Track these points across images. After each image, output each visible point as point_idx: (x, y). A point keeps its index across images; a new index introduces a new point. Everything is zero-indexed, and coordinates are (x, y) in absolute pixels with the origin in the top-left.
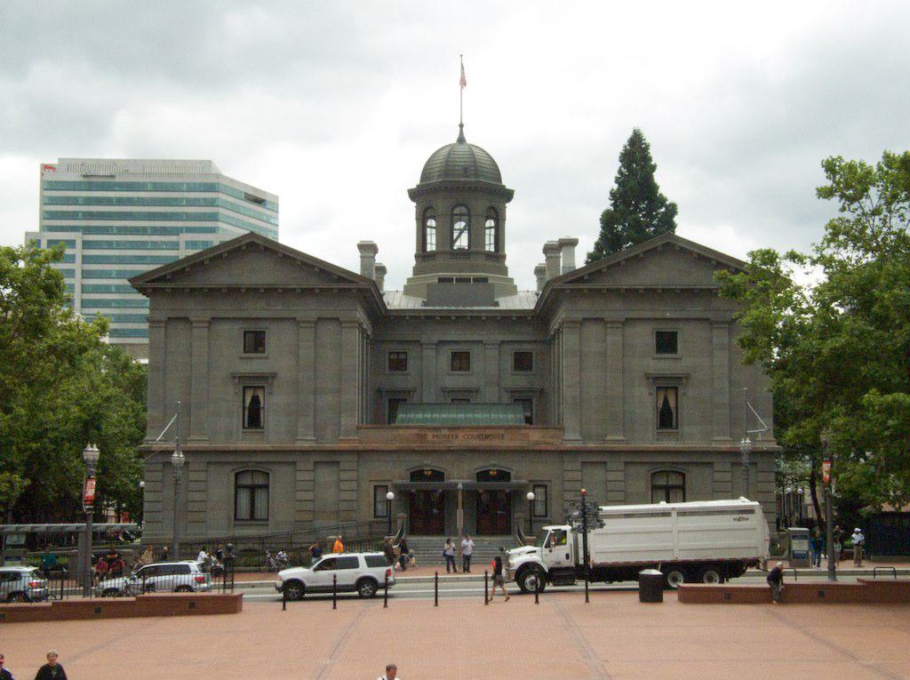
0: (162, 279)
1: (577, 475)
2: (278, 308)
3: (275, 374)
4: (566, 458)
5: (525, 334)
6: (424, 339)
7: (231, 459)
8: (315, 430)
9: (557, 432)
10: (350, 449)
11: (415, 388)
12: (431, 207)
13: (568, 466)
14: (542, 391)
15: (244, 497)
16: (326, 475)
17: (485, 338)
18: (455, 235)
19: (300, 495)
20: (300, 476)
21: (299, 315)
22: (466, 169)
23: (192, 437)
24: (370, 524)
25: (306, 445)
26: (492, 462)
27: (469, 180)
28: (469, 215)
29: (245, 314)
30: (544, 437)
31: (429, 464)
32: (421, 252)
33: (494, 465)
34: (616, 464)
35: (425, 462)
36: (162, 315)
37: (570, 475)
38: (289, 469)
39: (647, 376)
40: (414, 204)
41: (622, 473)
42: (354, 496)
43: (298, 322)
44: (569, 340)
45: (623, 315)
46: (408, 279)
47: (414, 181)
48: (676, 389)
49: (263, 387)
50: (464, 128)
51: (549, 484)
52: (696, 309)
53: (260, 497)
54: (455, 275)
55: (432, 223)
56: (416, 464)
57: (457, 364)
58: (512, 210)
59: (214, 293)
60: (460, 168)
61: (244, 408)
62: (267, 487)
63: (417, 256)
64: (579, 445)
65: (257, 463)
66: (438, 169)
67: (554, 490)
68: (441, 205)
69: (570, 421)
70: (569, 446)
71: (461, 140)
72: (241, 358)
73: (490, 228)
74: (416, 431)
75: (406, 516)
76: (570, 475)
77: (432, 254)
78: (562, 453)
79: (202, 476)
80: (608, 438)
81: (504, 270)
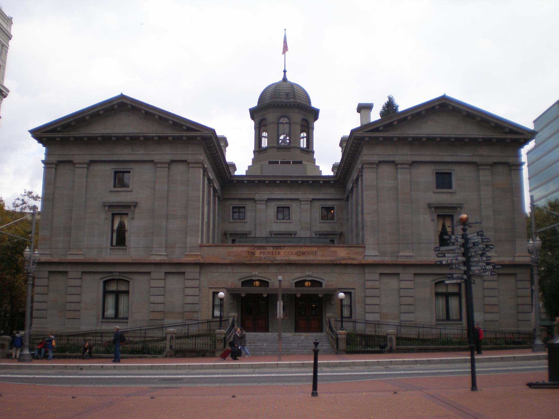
0: (54, 130)
1: (377, 284)
2: (140, 153)
3: (137, 203)
4: (367, 270)
5: (329, 193)
6: (257, 197)
7: (101, 269)
8: (166, 247)
9: (360, 250)
10: (193, 262)
11: (251, 232)
12: (265, 119)
13: (368, 276)
14: (341, 234)
15: (111, 300)
16: (174, 283)
17: (300, 196)
19: (153, 299)
20: (154, 283)
21: (156, 158)
22: (287, 95)
23: (71, 252)
24: (208, 322)
25: (158, 259)
26: (307, 273)
27: (289, 100)
28: (289, 123)
29: (115, 158)
30: (348, 254)
31: (257, 274)
32: (257, 149)
33: (309, 276)
34: (407, 274)
35: (253, 273)
36: (54, 159)
37: (369, 284)
38: (145, 278)
39: (430, 206)
41: (412, 282)
42: (196, 299)
43: (156, 163)
44: (368, 177)
45: (410, 159)
46: (249, 167)
47: (254, 104)
48: (451, 217)
49: (127, 214)
50: (287, 73)
51: (352, 291)
52: (465, 155)
53: (123, 300)
55: (265, 134)
56: (246, 275)
57: (281, 216)
58: (317, 125)
59: (92, 141)
60: (284, 94)
61: (112, 231)
62: (127, 292)
63: (254, 152)
64: (378, 259)
65: (120, 273)
66: (269, 95)
67: (358, 295)
68: (271, 117)
69: (369, 240)
70: (369, 260)
71: (285, 79)
72: (111, 191)
73: (303, 138)
74: (246, 249)
75: (236, 315)
76: (369, 284)
77: (266, 149)
78: (363, 266)
79: (78, 282)
80: (401, 254)
81: (314, 161)
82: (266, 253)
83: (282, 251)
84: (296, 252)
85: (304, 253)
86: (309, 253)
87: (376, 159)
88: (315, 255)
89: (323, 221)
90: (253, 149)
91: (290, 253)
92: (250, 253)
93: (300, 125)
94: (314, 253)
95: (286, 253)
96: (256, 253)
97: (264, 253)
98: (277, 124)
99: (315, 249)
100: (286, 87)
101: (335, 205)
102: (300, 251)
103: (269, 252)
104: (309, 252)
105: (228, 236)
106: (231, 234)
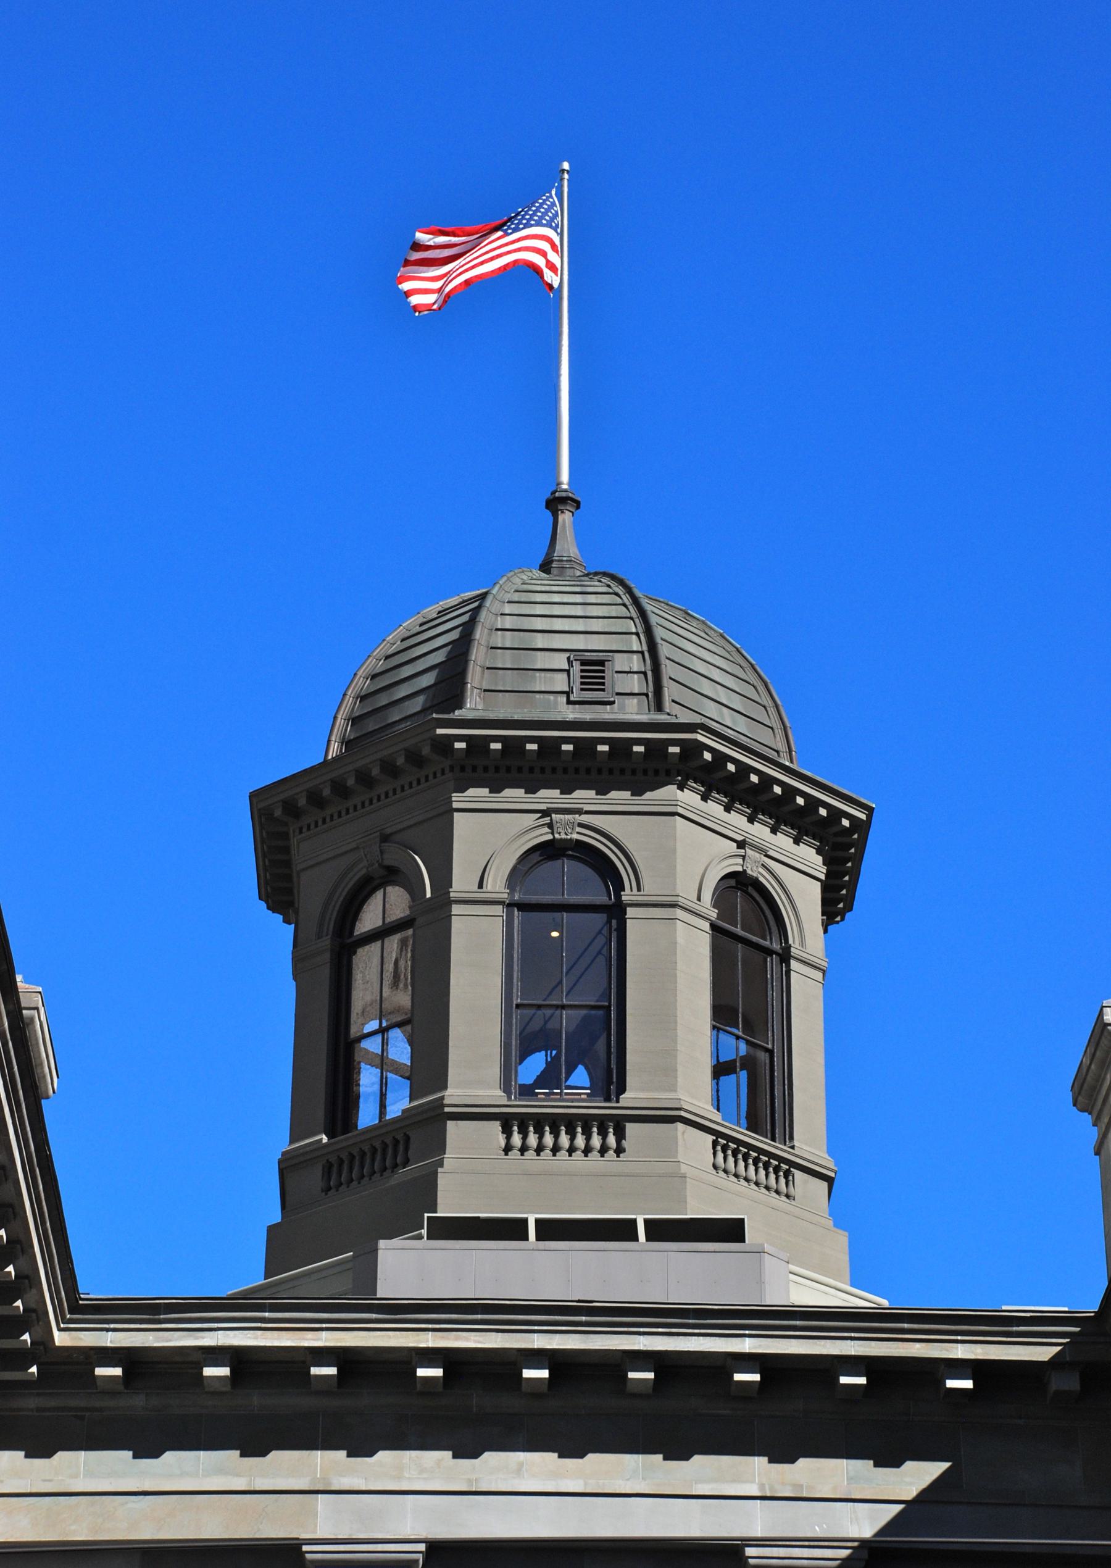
60: (560, 660)
93: (706, 926)
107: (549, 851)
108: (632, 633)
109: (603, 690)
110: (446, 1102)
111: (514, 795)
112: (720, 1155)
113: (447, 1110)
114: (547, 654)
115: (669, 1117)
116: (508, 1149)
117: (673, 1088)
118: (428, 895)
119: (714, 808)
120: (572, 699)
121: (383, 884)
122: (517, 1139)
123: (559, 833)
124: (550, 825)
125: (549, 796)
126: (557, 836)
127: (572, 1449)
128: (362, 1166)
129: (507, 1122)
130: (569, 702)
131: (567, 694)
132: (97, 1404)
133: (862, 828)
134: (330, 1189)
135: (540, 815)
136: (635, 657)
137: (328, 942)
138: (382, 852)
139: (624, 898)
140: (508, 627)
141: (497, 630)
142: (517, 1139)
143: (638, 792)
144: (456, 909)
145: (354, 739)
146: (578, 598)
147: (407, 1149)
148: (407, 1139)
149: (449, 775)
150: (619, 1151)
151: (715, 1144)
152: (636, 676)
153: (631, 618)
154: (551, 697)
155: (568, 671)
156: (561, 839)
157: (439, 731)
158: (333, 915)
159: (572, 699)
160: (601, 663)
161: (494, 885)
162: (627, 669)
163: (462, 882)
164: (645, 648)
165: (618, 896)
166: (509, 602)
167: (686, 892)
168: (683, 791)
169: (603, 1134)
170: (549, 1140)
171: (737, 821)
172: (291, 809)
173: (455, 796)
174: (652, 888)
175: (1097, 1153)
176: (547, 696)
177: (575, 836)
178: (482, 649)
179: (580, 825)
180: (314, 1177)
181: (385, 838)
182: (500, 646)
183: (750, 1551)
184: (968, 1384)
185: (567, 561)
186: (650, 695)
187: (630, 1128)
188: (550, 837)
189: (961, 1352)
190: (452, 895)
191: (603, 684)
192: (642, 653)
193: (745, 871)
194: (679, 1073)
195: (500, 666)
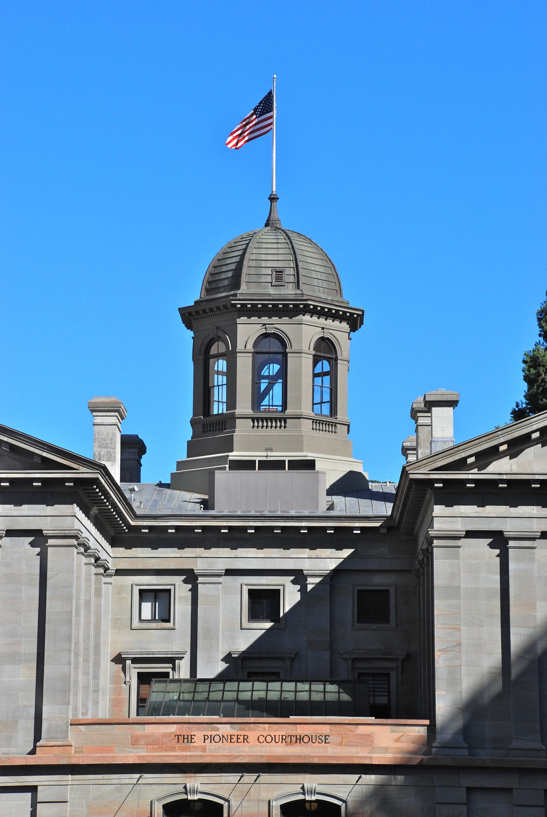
18: (263, 386)
22: (279, 274)
40: (191, 334)
54: (258, 456)
60: (269, 271)
74: (173, 728)
80: (515, 744)
82: (217, 739)
83: (253, 733)
84: (282, 736)
85: (300, 739)
86: (310, 739)
87: (460, 526)
88: (325, 743)
89: (360, 625)
90: (190, 414)
91: (269, 739)
92: (181, 739)
94: (323, 739)
95: (262, 739)
96: (195, 739)
97: (212, 739)
98: (251, 355)
99: (325, 730)
100: (275, 251)
101: (390, 585)
102: (293, 733)
103: (223, 736)
104: (312, 736)
105: (128, 662)
106: (135, 661)
107: (265, 336)
108: (291, 260)
109: (282, 281)
110: (236, 414)
111: (254, 319)
112: (315, 424)
113: (236, 416)
114: (265, 268)
115: (299, 417)
116: (253, 427)
117: (300, 409)
118: (230, 349)
119: (315, 318)
120: (273, 285)
121: (218, 341)
122: (256, 424)
123: (268, 331)
124: (265, 328)
125: (265, 319)
126: (268, 332)
127: (260, 547)
128: (213, 427)
129: (253, 419)
130: (272, 286)
131: (271, 283)
132: (142, 536)
133: (362, 316)
134: (204, 432)
135: (262, 325)
136: (292, 269)
137: (202, 357)
138: (217, 332)
139: (287, 351)
140: (254, 259)
141: (251, 260)
142: (256, 424)
143: (291, 318)
144: (238, 355)
145: (209, 289)
146: (275, 246)
147: (225, 425)
148: (226, 421)
149: (236, 313)
150: (285, 427)
151: (313, 422)
152: (292, 276)
153: (291, 254)
154: (266, 284)
155: (272, 275)
156: (269, 333)
157: (232, 302)
158: (203, 349)
159: (273, 285)
160: (282, 272)
161: (249, 348)
162: (289, 274)
163: (240, 346)
164: (295, 266)
165: (285, 350)
166: (255, 248)
167: (305, 348)
168: (304, 316)
169: (281, 422)
170: (265, 424)
171: (322, 320)
172: (190, 314)
173: (238, 320)
174: (295, 348)
175: (416, 432)
176: (265, 283)
177: (273, 331)
178: (246, 267)
179: (274, 328)
180: (200, 427)
181: (218, 328)
182: (251, 266)
183: (304, 572)
184: (359, 532)
185: (275, 220)
186: (296, 283)
187: (288, 421)
188: (265, 332)
189: (357, 525)
190: (237, 350)
191: (282, 279)
192: (294, 268)
193: (324, 336)
194: (302, 404)
195: (251, 273)
